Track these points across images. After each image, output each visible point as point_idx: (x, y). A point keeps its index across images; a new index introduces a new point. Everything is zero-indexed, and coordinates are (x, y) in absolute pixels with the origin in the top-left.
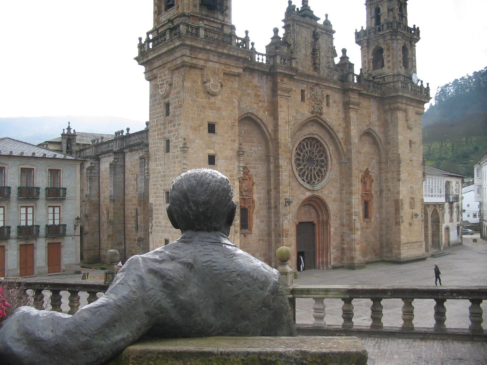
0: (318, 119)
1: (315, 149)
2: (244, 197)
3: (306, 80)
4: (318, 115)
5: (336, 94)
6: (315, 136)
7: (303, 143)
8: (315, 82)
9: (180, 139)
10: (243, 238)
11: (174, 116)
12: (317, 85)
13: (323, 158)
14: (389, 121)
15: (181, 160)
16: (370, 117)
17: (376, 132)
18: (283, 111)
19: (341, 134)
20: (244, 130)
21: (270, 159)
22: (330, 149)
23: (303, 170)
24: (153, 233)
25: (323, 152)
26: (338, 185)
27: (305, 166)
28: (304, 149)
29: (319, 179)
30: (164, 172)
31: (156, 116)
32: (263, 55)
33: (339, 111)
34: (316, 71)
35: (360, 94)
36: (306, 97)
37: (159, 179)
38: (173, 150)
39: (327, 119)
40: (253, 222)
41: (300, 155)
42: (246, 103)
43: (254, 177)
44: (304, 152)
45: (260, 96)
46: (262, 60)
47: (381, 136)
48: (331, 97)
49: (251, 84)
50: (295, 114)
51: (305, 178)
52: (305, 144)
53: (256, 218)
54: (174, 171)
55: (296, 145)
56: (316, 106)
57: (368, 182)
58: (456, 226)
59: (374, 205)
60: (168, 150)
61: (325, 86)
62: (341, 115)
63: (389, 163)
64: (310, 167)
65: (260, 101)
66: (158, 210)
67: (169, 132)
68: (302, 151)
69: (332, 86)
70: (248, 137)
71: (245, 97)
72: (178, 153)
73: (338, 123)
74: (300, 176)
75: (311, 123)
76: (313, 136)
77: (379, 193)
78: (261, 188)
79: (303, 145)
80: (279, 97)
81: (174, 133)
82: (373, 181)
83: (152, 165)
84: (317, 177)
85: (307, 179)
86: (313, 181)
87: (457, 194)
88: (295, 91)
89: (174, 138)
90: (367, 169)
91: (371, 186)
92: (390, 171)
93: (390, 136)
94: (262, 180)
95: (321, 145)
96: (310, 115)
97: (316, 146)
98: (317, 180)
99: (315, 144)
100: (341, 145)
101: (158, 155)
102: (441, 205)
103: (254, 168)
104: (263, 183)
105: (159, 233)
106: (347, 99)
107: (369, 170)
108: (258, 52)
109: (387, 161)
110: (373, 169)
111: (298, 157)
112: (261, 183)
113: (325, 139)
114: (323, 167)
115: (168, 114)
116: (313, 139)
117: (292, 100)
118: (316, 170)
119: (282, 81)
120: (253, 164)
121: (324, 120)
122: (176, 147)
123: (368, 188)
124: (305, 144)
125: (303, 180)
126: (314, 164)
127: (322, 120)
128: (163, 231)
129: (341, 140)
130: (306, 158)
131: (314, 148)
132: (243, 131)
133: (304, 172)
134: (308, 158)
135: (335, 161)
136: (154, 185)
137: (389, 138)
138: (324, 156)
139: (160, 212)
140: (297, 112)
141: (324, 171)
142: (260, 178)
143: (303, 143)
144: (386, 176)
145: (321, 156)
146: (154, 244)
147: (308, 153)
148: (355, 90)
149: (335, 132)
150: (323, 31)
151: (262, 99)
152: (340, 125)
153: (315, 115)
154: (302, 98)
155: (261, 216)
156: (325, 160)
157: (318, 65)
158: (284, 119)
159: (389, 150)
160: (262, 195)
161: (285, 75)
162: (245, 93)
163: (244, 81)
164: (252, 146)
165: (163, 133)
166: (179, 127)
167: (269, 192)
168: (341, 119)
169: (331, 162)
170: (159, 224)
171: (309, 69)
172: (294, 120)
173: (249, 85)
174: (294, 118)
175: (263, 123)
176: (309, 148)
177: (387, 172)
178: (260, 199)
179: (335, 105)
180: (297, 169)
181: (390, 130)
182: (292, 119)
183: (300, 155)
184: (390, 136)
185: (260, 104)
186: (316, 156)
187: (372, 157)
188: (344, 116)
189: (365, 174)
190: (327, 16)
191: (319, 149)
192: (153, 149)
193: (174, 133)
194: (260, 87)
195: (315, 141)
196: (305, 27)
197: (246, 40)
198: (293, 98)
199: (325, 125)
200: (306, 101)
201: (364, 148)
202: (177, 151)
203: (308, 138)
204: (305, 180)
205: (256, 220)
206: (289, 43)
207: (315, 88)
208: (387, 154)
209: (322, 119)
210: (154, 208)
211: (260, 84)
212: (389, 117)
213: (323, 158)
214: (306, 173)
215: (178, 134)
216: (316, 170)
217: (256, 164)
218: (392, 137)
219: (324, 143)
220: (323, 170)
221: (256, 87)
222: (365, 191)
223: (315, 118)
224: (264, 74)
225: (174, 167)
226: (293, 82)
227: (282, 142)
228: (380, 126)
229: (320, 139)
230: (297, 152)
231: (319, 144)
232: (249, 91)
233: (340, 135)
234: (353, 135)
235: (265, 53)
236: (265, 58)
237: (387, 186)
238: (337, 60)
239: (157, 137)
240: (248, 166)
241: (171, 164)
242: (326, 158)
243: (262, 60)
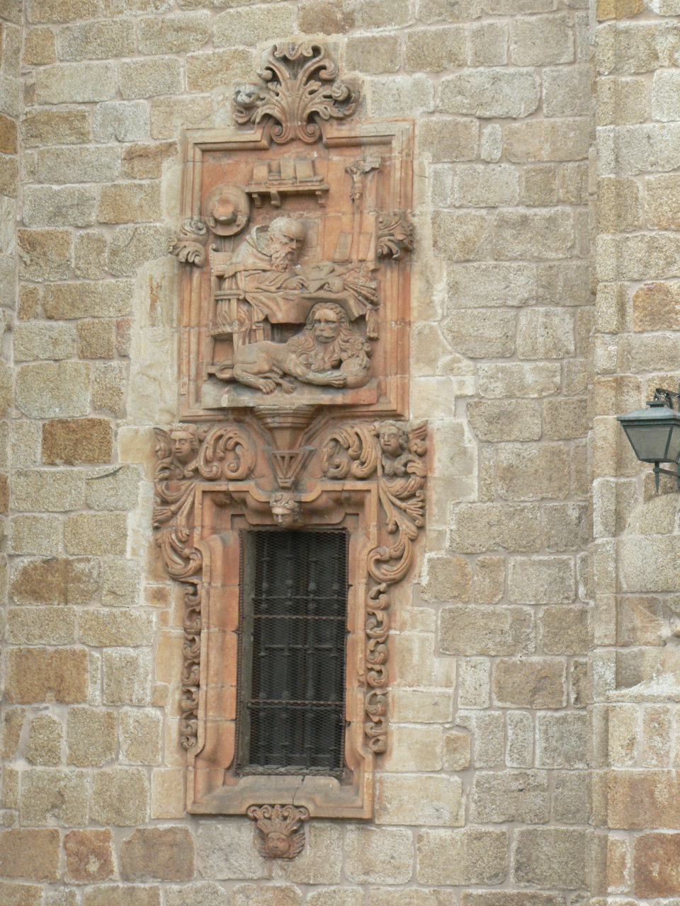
2: (247, 399)
10: (247, 859)
40: (398, 691)
43: (425, 161)
53: (446, 648)
104: (552, 220)
112: (524, 221)
142: (509, 179)
155: (520, 620)
160: (529, 373)
205: (439, 666)
240: (339, 40)
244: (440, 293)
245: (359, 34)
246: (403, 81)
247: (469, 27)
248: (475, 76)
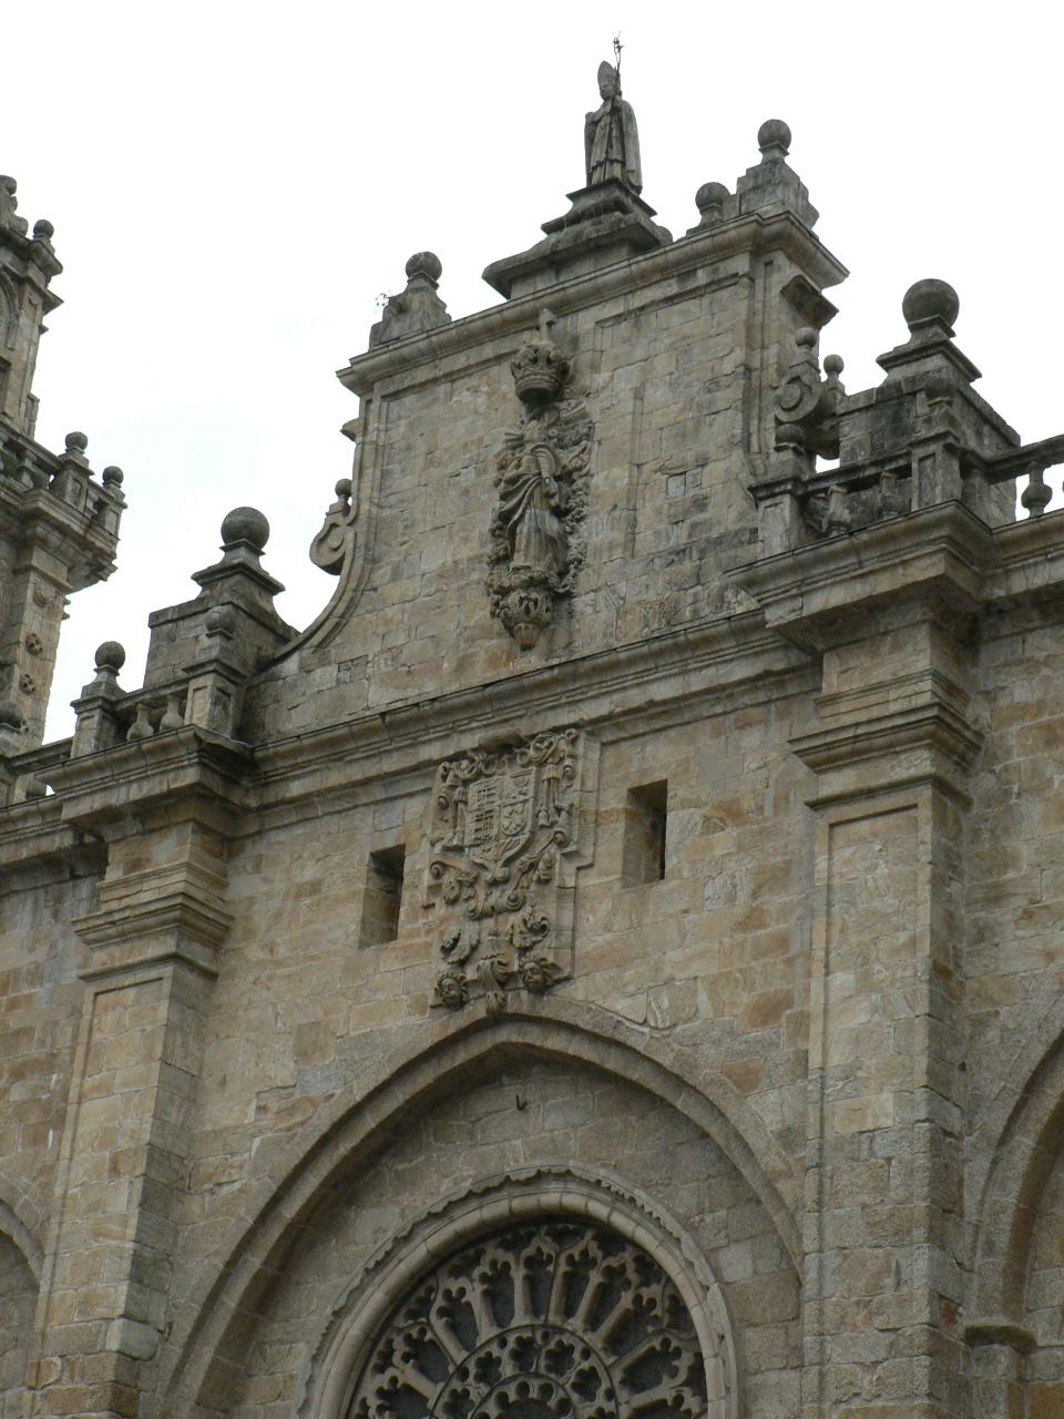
0: (534, 1037)
1: (576, 1323)
3: (390, 764)
4: (520, 1001)
7: (453, 1285)
8: (469, 741)
12: (505, 749)
18: (104, 1089)
19: (772, 1097)
34: (526, 648)
39: (621, 1005)
45: (27, 1032)
50: (283, 1072)
52: (475, 1295)
56: (470, 932)
61: (594, 726)
65: (18, 1074)
69: (663, 690)
73: (746, 999)
75: (512, 1090)
76: (523, 1202)
88: (315, 887)
95: (649, 1268)
96: (427, 1029)
97: (595, 1278)
99: (587, 1261)
116: (564, 1223)
117: (279, 964)
121: (584, 1021)
127: (573, 1029)
131: (569, 1311)
140: (307, 1046)
143: (453, 1285)
147: (507, 1369)
148: (873, 607)
149: (713, 1093)
150: (637, 301)
158: (106, 1138)
161: (152, 814)
171: (462, 665)
179: (724, 841)
186: (586, 1384)
190: (775, 138)
191: (626, 1300)
194: (36, 976)
195: (588, 1241)
196: (466, 372)
198: (282, 951)
199: (613, 1062)
203: (512, 1231)
209: (567, 1016)
211: (41, 953)
223: (507, 1035)
224: (74, 877)
226: (299, 831)
227: (55, 1327)
229: (599, 1209)
231: (627, 1256)
234: (836, 1059)
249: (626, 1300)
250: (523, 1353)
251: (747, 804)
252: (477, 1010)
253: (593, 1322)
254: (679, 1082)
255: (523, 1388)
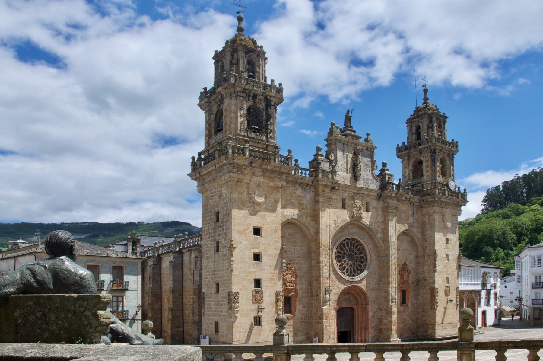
1: (355, 248)
5: (376, 201)
6: (355, 237)
9: (228, 241)
11: (223, 222)
13: (362, 255)
14: (427, 222)
15: (229, 258)
16: (408, 219)
17: (415, 233)
20: (288, 233)
21: (312, 256)
22: (368, 247)
23: (344, 265)
24: (205, 316)
25: (362, 250)
26: (377, 277)
27: (345, 261)
28: (345, 247)
29: (358, 272)
30: (214, 267)
31: (208, 222)
32: (306, 170)
33: (378, 215)
35: (398, 200)
36: (346, 204)
37: (210, 273)
38: (222, 249)
41: (340, 253)
42: (289, 211)
44: (345, 251)
45: (304, 204)
46: (305, 174)
47: (419, 235)
48: (370, 204)
49: (294, 195)
51: (345, 271)
52: (345, 244)
54: (223, 266)
55: (337, 244)
57: (406, 274)
58: (494, 310)
59: (410, 295)
60: (218, 250)
62: (381, 219)
63: (426, 257)
64: (350, 262)
65: (303, 209)
66: (209, 298)
67: (219, 235)
68: (342, 249)
70: (292, 238)
71: (289, 205)
72: (226, 252)
74: (340, 270)
75: (351, 226)
76: (352, 237)
77: (416, 283)
78: (304, 280)
79: (344, 244)
80: (320, 204)
81: (223, 236)
82: (410, 273)
83: (205, 262)
84: (356, 271)
85: (347, 272)
86: (353, 274)
87: (495, 282)
88: (336, 199)
89: (223, 240)
90: (405, 263)
91: (408, 277)
92: (427, 264)
93: (427, 235)
94: (305, 273)
95: (361, 244)
97: (356, 245)
98: (356, 273)
100: (379, 243)
101: (210, 254)
102: (478, 293)
103: (297, 264)
105: (210, 316)
106: (386, 204)
107: (407, 264)
108: (301, 167)
109: (424, 256)
110: (410, 262)
111: (338, 254)
113: (364, 239)
114: (362, 262)
115: (217, 220)
116: (353, 239)
118: (356, 265)
119: (323, 191)
120: (296, 260)
122: (225, 247)
123: (405, 279)
124: (345, 244)
125: (344, 273)
126: (354, 260)
128: (213, 315)
129: (379, 240)
130: (347, 255)
131: (354, 247)
132: (287, 233)
133: (345, 267)
134: (348, 255)
135: (374, 257)
136: (206, 278)
137: (426, 236)
138: (364, 253)
139: (211, 299)
141: (364, 265)
143: (344, 242)
144: (423, 269)
145: (361, 253)
146: (206, 325)
147: (349, 251)
151: (305, 207)
152: (379, 227)
153: (355, 219)
154: (342, 205)
156: (364, 256)
157: (359, 177)
159: (426, 247)
162: (289, 202)
163: (289, 192)
164: (296, 246)
165: (215, 236)
166: (227, 231)
167: (310, 284)
168: (380, 222)
169: (370, 258)
170: (210, 310)
172: (334, 224)
173: (292, 196)
174: (335, 222)
175: (306, 227)
176: (350, 247)
177: (424, 266)
178: (302, 289)
180: (337, 265)
181: (427, 230)
182: (333, 223)
183: (340, 253)
184: (427, 235)
185: (303, 211)
186: (356, 254)
187: (410, 252)
188: (383, 220)
189: (402, 267)
190: (368, 134)
191: (359, 247)
192: (205, 249)
193: (223, 236)
195: (355, 241)
197: (287, 160)
198: (334, 205)
200: (346, 208)
201: (402, 246)
202: (226, 251)
203: (349, 239)
204: (345, 273)
206: (331, 159)
207: (355, 196)
208: (424, 250)
210: (206, 296)
212: (426, 219)
213: (362, 255)
214: (347, 267)
215: (227, 236)
216: (356, 265)
217: (299, 260)
218: (428, 236)
219: (363, 243)
220: (362, 264)
221: (299, 197)
222: (402, 282)
225: (223, 263)
228: (417, 227)
229: (359, 239)
230: (337, 250)
231: (359, 243)
232: (293, 201)
233: (379, 235)
235: (308, 168)
236: (308, 172)
237: (424, 277)
238: (377, 172)
239: (208, 239)
241: (221, 261)
242: (365, 254)
243: (305, 174)
244: (298, 280)
245: (293, 262)
246: (295, 265)
247: (300, 262)
248: (300, 265)
249: (359, 247)
250: (350, 250)
251: (376, 207)
252: (354, 219)
253: (356, 248)
254: (371, 230)
255: (350, 253)
